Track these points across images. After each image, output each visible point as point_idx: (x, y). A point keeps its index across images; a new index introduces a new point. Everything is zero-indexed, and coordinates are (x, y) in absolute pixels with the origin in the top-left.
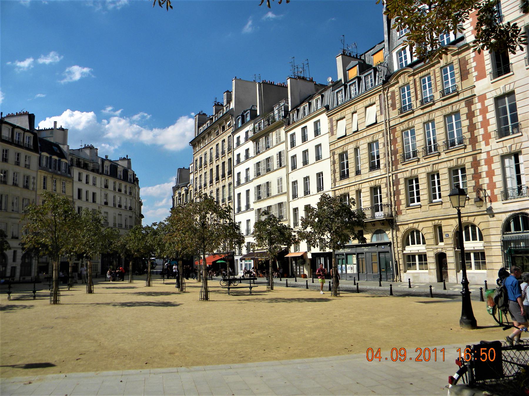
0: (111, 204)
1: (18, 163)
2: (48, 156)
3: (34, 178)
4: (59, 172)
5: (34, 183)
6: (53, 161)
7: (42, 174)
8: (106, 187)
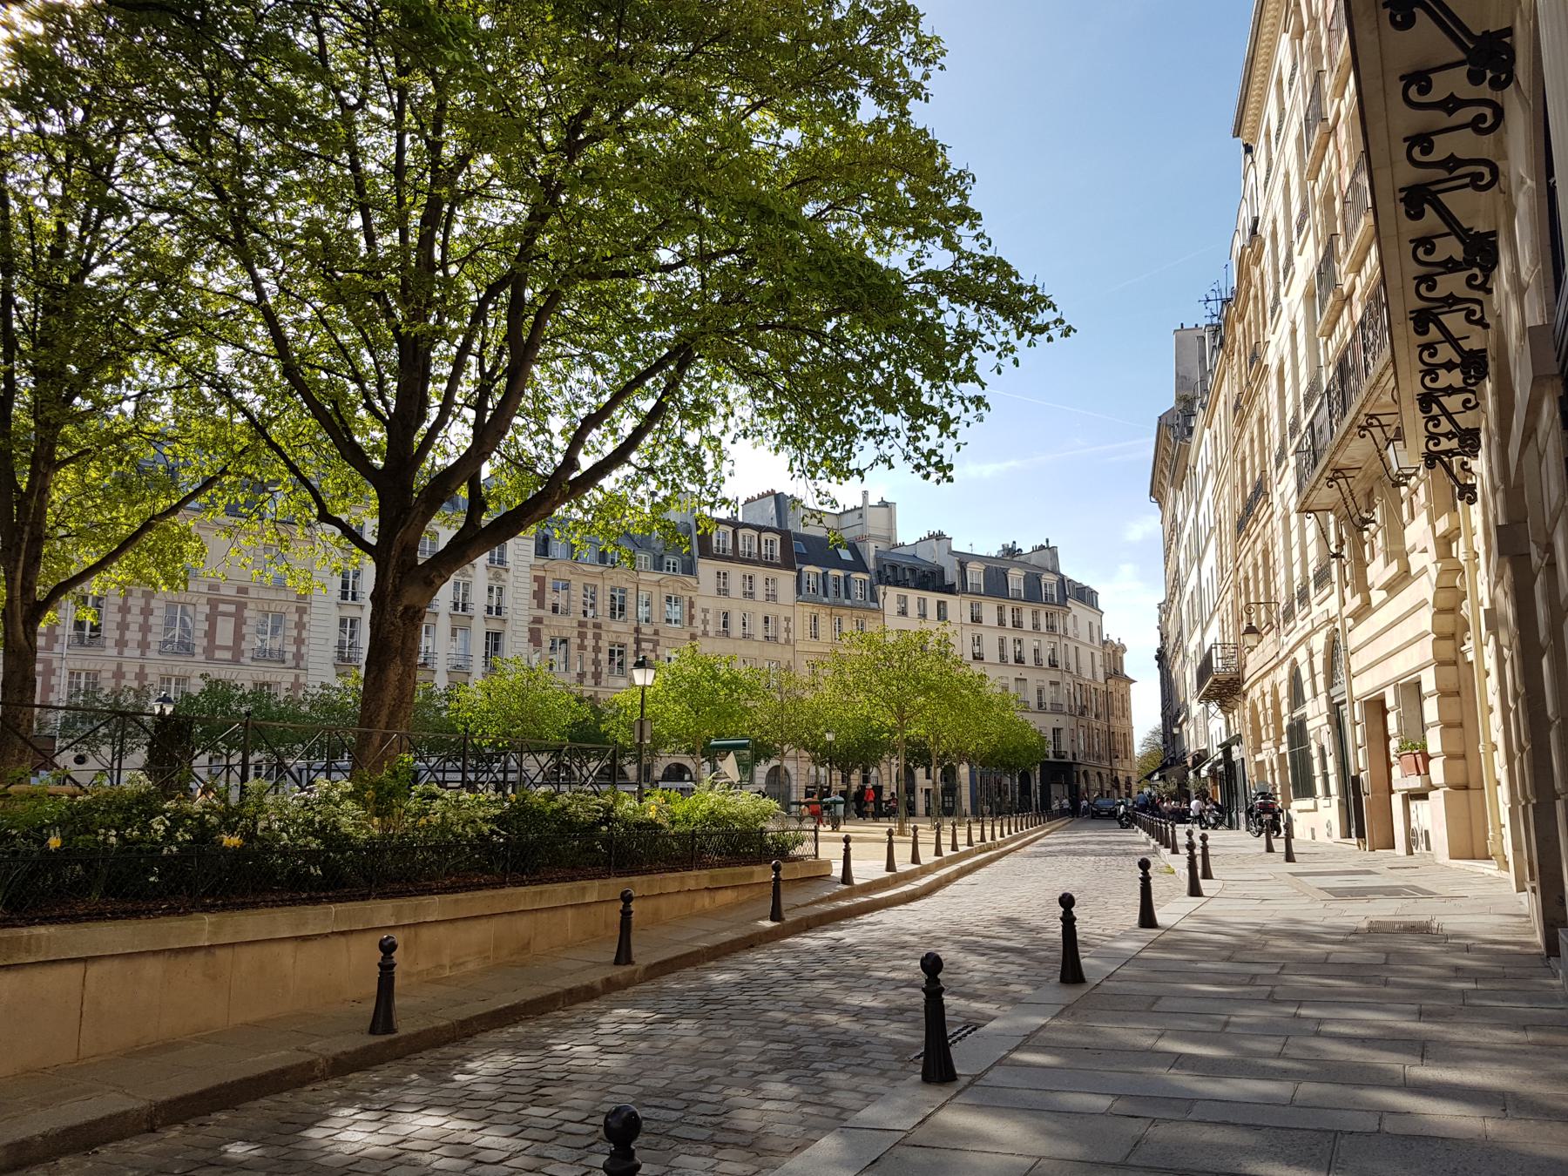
0: (991, 654)
1: (749, 595)
2: (820, 571)
3: (787, 620)
4: (847, 602)
5: (788, 630)
6: (830, 581)
7: (808, 610)
8: (976, 619)
